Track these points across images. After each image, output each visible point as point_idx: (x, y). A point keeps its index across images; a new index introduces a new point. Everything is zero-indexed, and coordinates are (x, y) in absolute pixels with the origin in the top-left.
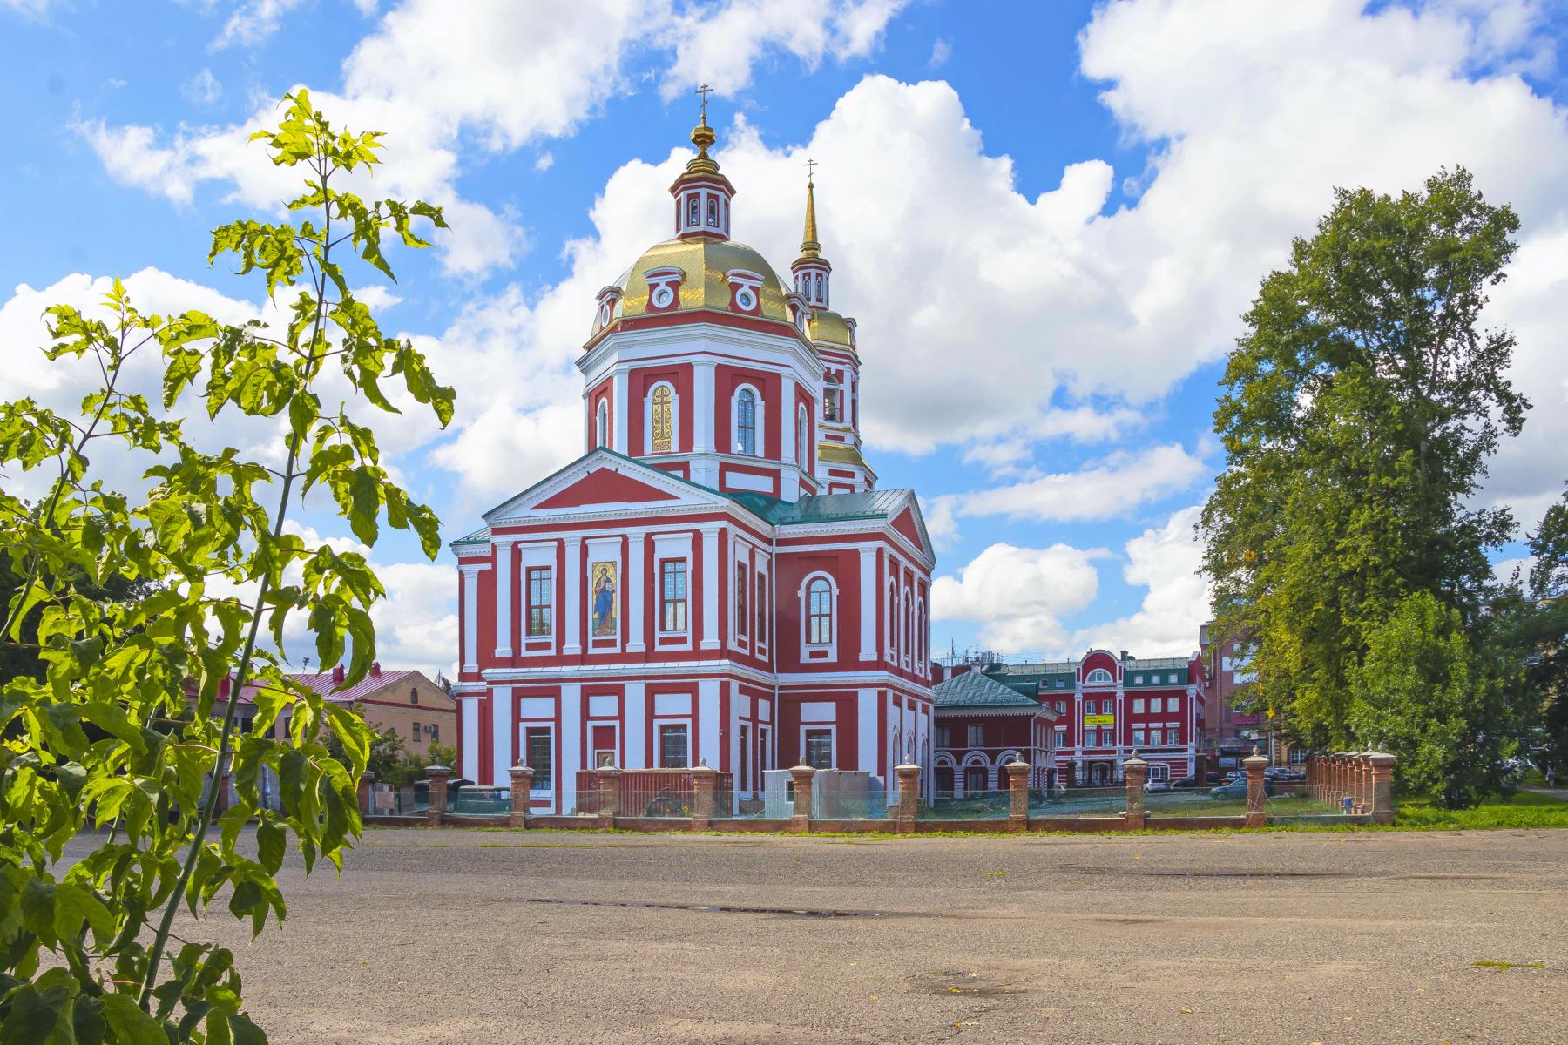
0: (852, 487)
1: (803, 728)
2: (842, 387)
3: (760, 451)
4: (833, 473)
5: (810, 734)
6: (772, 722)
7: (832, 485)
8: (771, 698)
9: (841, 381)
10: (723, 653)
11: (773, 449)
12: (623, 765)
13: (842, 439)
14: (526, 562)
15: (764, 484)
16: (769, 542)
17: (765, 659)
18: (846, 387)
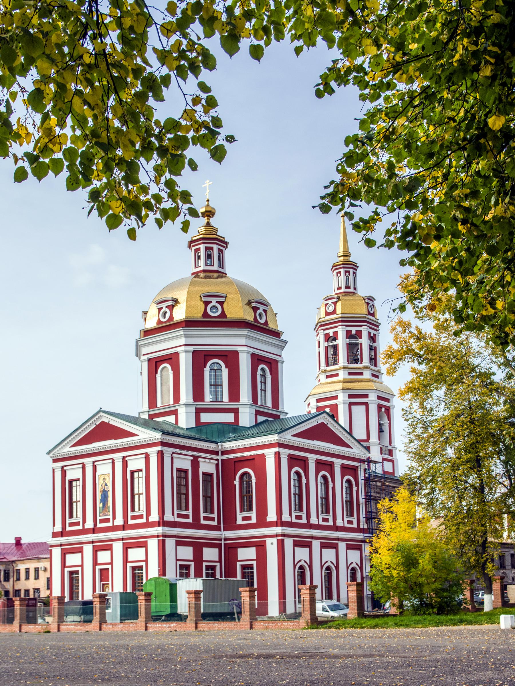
0: (366, 404)
1: (239, 564)
2: (360, 341)
3: (226, 398)
4: (350, 396)
5: (243, 567)
6: (220, 561)
7: (351, 404)
8: (219, 546)
9: (361, 337)
10: (162, 523)
11: (234, 395)
12: (112, 590)
13: (361, 374)
14: (68, 478)
15: (229, 418)
16: (216, 453)
17: (215, 523)
18: (365, 341)
